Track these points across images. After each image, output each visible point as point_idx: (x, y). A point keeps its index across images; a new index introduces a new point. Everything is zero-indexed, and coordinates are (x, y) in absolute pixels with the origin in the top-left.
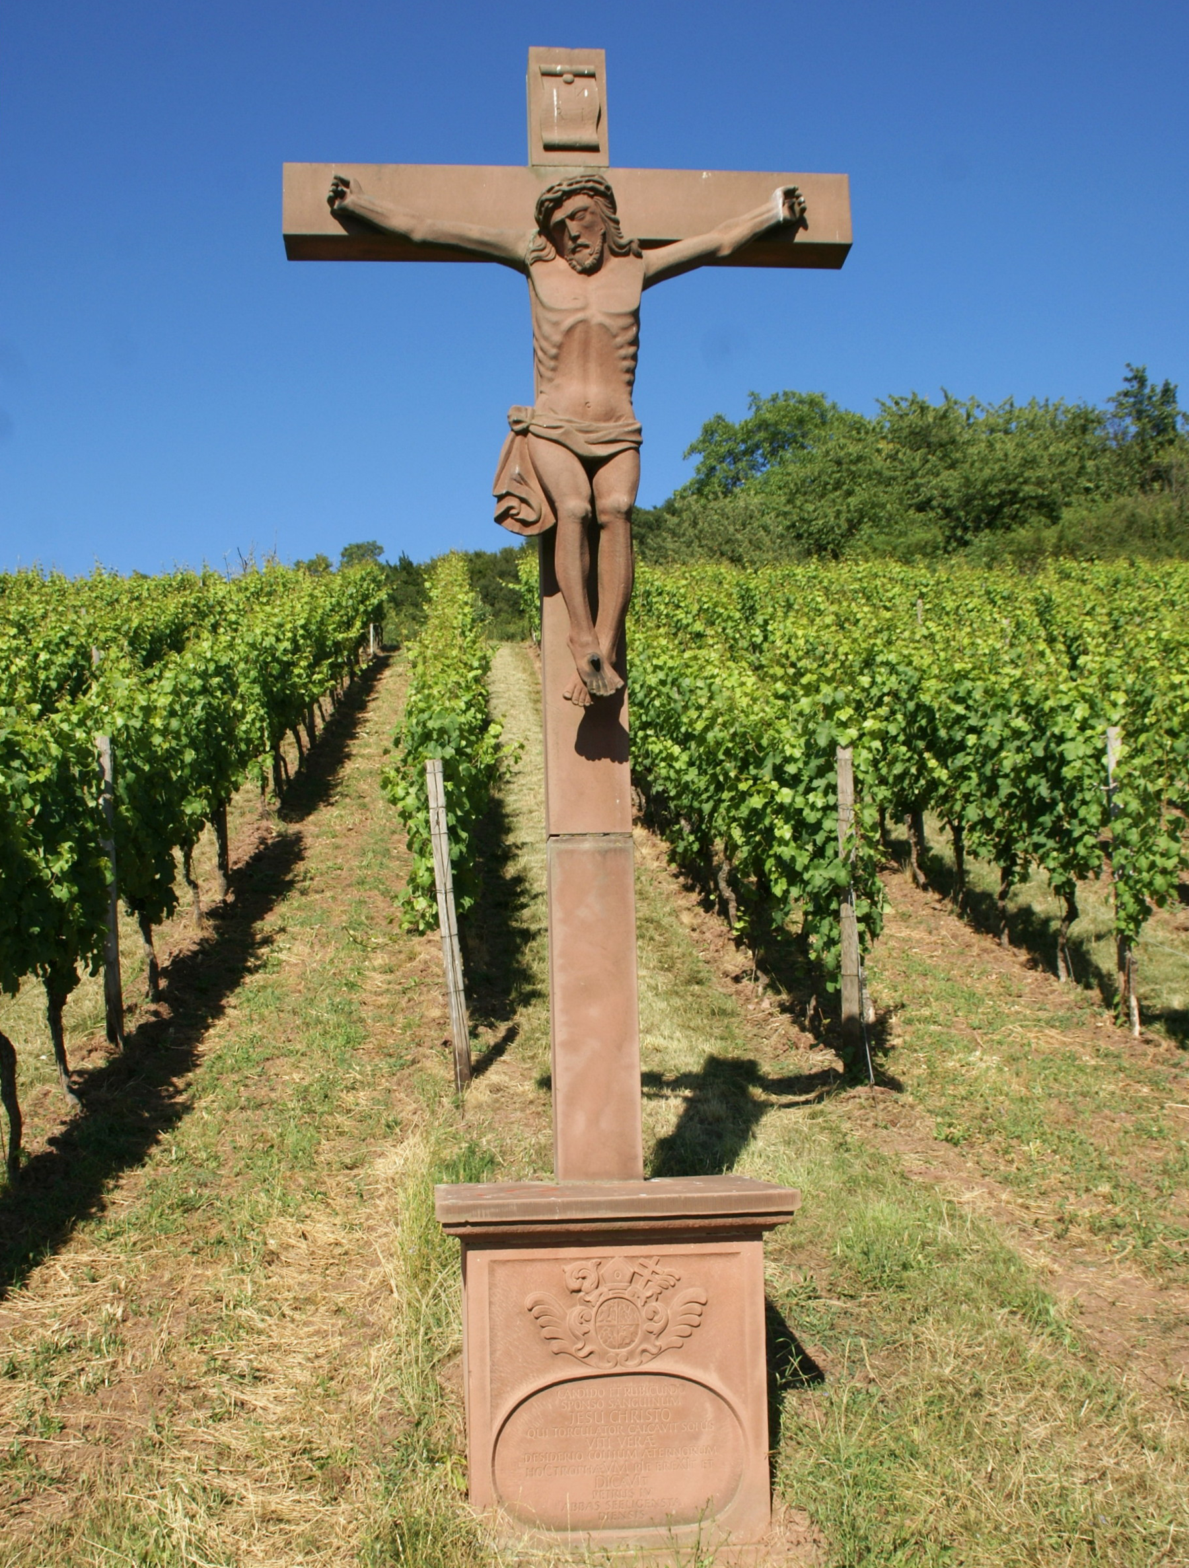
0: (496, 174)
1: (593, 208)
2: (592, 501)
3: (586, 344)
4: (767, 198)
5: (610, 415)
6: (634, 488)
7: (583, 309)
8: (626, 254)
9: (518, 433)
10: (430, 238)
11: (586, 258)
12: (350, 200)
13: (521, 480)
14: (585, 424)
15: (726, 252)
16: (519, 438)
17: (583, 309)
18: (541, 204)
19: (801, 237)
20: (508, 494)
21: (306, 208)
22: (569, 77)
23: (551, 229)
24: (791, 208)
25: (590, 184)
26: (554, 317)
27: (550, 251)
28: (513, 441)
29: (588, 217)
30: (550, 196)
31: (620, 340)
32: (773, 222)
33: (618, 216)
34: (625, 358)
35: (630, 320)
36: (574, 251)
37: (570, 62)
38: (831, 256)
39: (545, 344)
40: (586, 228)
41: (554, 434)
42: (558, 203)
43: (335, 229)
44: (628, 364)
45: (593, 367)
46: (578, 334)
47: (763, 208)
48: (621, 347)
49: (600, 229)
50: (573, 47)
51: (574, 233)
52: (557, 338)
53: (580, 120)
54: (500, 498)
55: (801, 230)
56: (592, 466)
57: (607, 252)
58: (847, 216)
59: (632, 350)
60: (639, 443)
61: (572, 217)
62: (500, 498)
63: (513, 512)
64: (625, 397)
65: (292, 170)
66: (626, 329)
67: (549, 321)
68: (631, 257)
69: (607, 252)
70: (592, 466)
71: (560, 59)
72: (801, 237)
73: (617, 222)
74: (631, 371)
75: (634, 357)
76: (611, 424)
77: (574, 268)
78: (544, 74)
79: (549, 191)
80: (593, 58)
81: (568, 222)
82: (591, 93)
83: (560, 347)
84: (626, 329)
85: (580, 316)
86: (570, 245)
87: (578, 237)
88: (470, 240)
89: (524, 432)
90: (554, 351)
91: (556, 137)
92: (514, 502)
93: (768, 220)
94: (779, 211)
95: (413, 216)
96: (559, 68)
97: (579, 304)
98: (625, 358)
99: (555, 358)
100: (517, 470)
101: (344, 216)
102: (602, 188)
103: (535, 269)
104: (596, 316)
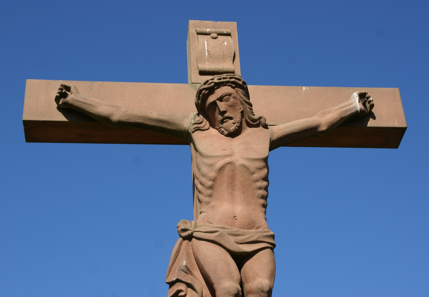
0: (169, 88)
1: (235, 94)
2: (241, 284)
3: (232, 178)
4: (349, 97)
5: (251, 225)
6: (273, 276)
7: (230, 156)
8: (257, 126)
9: (184, 238)
10: (123, 119)
11: (230, 125)
12: (71, 98)
13: (188, 271)
14: (234, 230)
15: (323, 128)
16: (186, 242)
17: (230, 156)
18: (200, 92)
19: (371, 123)
20: (178, 281)
21: (40, 101)
22: (215, 35)
23: (206, 109)
24: (364, 104)
25: (233, 80)
26: (209, 161)
27: (206, 124)
28: (181, 244)
29: (232, 100)
30: (206, 86)
31: (256, 176)
32: (353, 111)
33: (251, 101)
34: (260, 188)
35: (262, 164)
36: (222, 122)
37: (215, 28)
38: (391, 137)
39: (203, 180)
40: (231, 106)
41: (211, 236)
42: (211, 90)
43: (60, 117)
44: (262, 192)
45: (238, 194)
46: (226, 170)
47: (346, 103)
48: (258, 181)
49: (240, 108)
50: (216, 21)
51: (222, 110)
52: (212, 174)
53: (223, 58)
54: (171, 284)
55: (371, 119)
56: (241, 259)
57: (244, 124)
58: (401, 111)
59: (265, 183)
60: (274, 245)
61: (221, 99)
62: (171, 284)
63: (181, 294)
64: (262, 214)
65: (32, 85)
66: (260, 169)
67: (206, 164)
68: (261, 127)
69: (244, 124)
70: (241, 259)
71: (208, 26)
72: (371, 123)
73: (251, 105)
74: (265, 197)
75: (266, 188)
76: (253, 230)
77: (222, 133)
78: (199, 34)
79: (205, 84)
80: (231, 26)
81: (218, 102)
82: (231, 44)
83: (214, 180)
84: (260, 169)
85: (228, 160)
86: (220, 117)
87: (225, 112)
88: (151, 119)
89: (190, 238)
90: (210, 183)
91: (207, 66)
92: (182, 287)
93: (350, 109)
94: (356, 105)
95: (113, 106)
96: (208, 30)
97: (227, 152)
98: (260, 188)
99: (211, 187)
100: (184, 263)
101: (66, 108)
102: (241, 83)
103: (196, 136)
104: (239, 159)
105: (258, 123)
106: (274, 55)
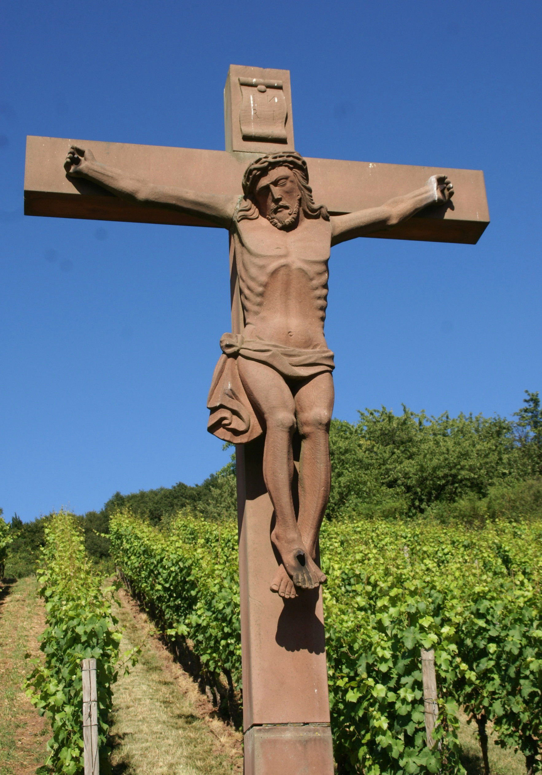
1: (292, 178)
2: (296, 414)
3: (287, 284)
5: (308, 343)
6: (331, 405)
8: (317, 217)
9: (229, 356)
10: (152, 198)
11: (286, 217)
12: (84, 165)
13: (233, 395)
14: (290, 349)
15: (394, 221)
16: (230, 360)
18: (249, 172)
19: (449, 215)
20: (222, 406)
22: (263, 88)
24: (442, 192)
25: (291, 159)
26: (260, 262)
27: (254, 211)
28: (225, 362)
29: (289, 184)
30: (258, 166)
31: (315, 282)
32: (430, 200)
34: (319, 298)
35: (322, 268)
36: (276, 211)
37: (263, 77)
38: (469, 232)
39: (252, 284)
40: (287, 192)
41: (262, 356)
42: (264, 171)
43: (70, 189)
44: (321, 302)
45: (293, 303)
47: (422, 190)
48: (317, 288)
49: (298, 195)
50: (264, 68)
51: (277, 196)
52: (263, 278)
53: (272, 120)
54: (213, 410)
55: (449, 210)
56: (295, 384)
57: (302, 215)
58: (484, 201)
59: (324, 291)
60: (333, 367)
61: (275, 183)
62: (213, 410)
63: (225, 422)
64: (320, 329)
66: (320, 274)
69: (302, 215)
70: (295, 384)
71: (254, 74)
72: (449, 215)
73: (310, 190)
74: (323, 309)
75: (325, 298)
76: (310, 350)
77: (275, 225)
78: (242, 84)
79: (257, 162)
80: (282, 76)
81: (272, 187)
82: (281, 100)
83: (265, 285)
84: (320, 274)
85: (282, 261)
86: (273, 206)
87: (280, 200)
88: (186, 201)
89: (235, 355)
90: (260, 289)
91: (253, 130)
92: (226, 414)
94: (435, 194)
96: (254, 80)
97: (282, 252)
98: (319, 298)
99: (261, 295)
100: (230, 386)
101: (78, 179)
102: (300, 162)
103: (242, 226)
104: (296, 261)
105: (315, 214)
106: (334, 118)
